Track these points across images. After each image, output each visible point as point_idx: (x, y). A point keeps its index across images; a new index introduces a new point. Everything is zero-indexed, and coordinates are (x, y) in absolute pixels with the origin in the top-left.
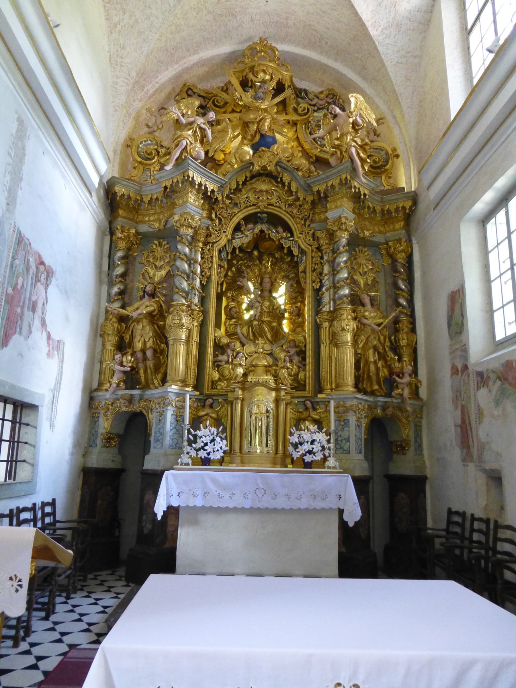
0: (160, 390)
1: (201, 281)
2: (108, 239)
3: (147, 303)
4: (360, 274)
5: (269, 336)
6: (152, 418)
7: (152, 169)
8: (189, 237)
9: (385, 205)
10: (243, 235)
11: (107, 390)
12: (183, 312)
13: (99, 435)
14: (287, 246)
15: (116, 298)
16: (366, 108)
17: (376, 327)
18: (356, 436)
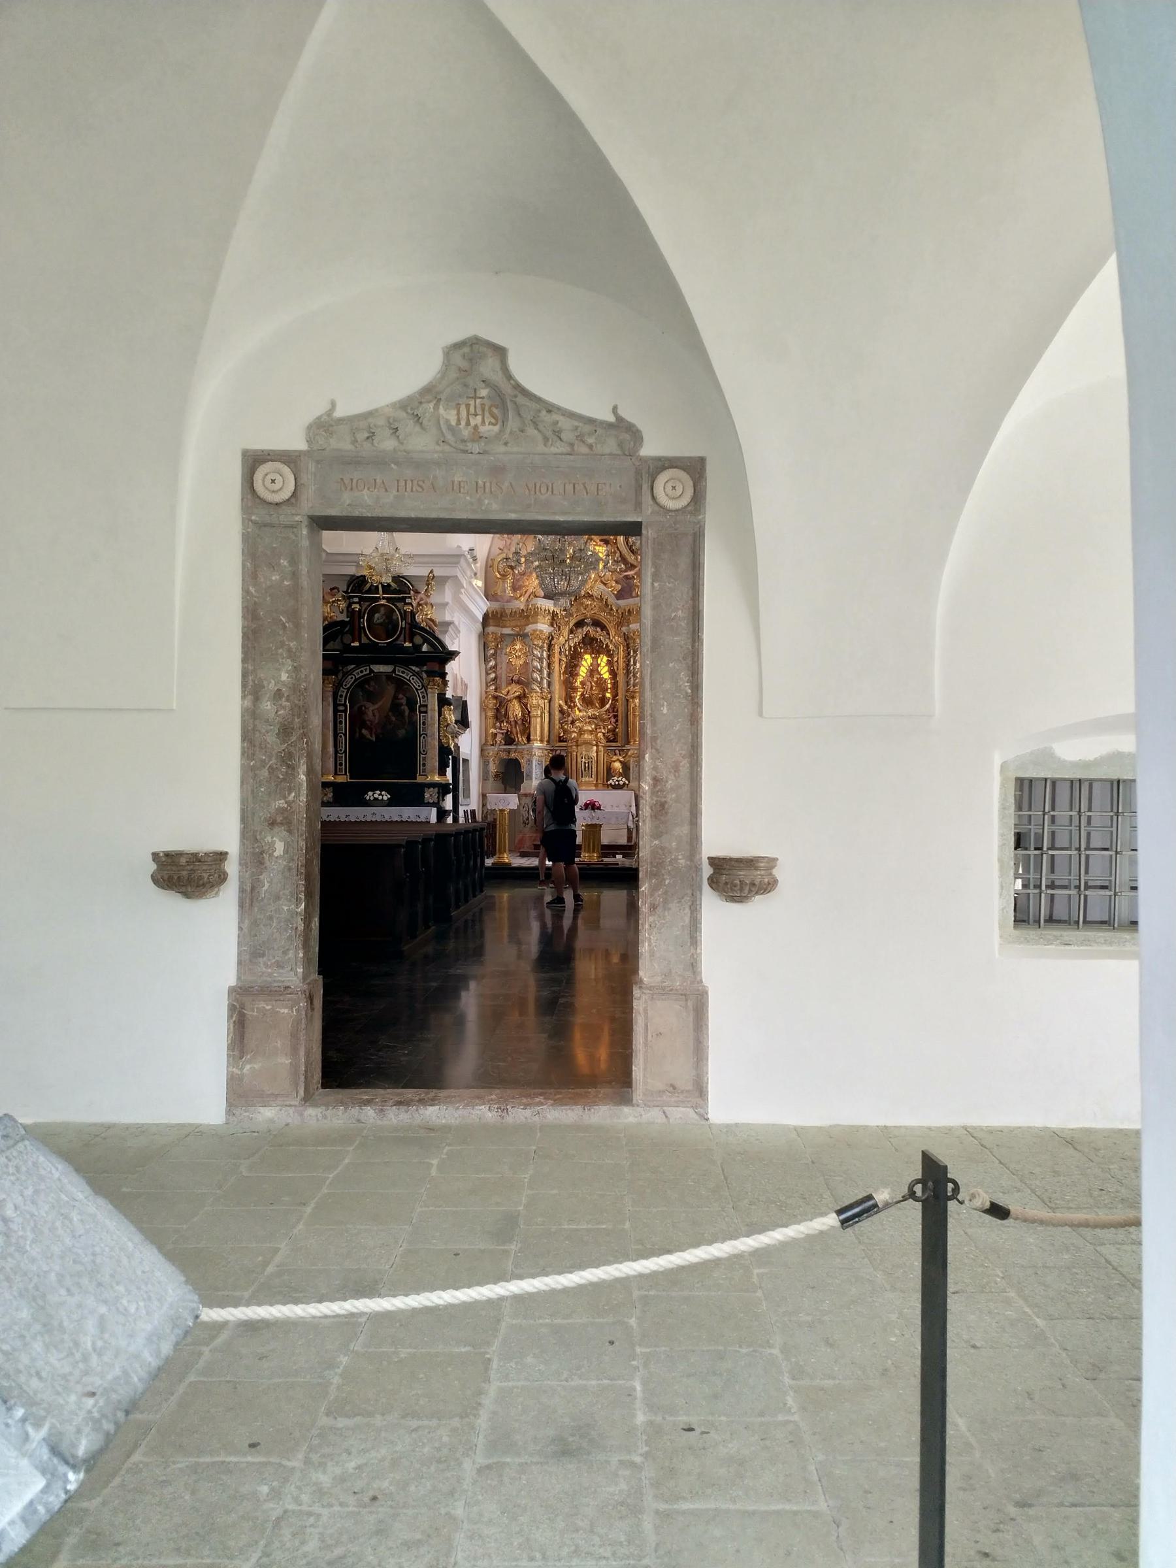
6: (523, 762)
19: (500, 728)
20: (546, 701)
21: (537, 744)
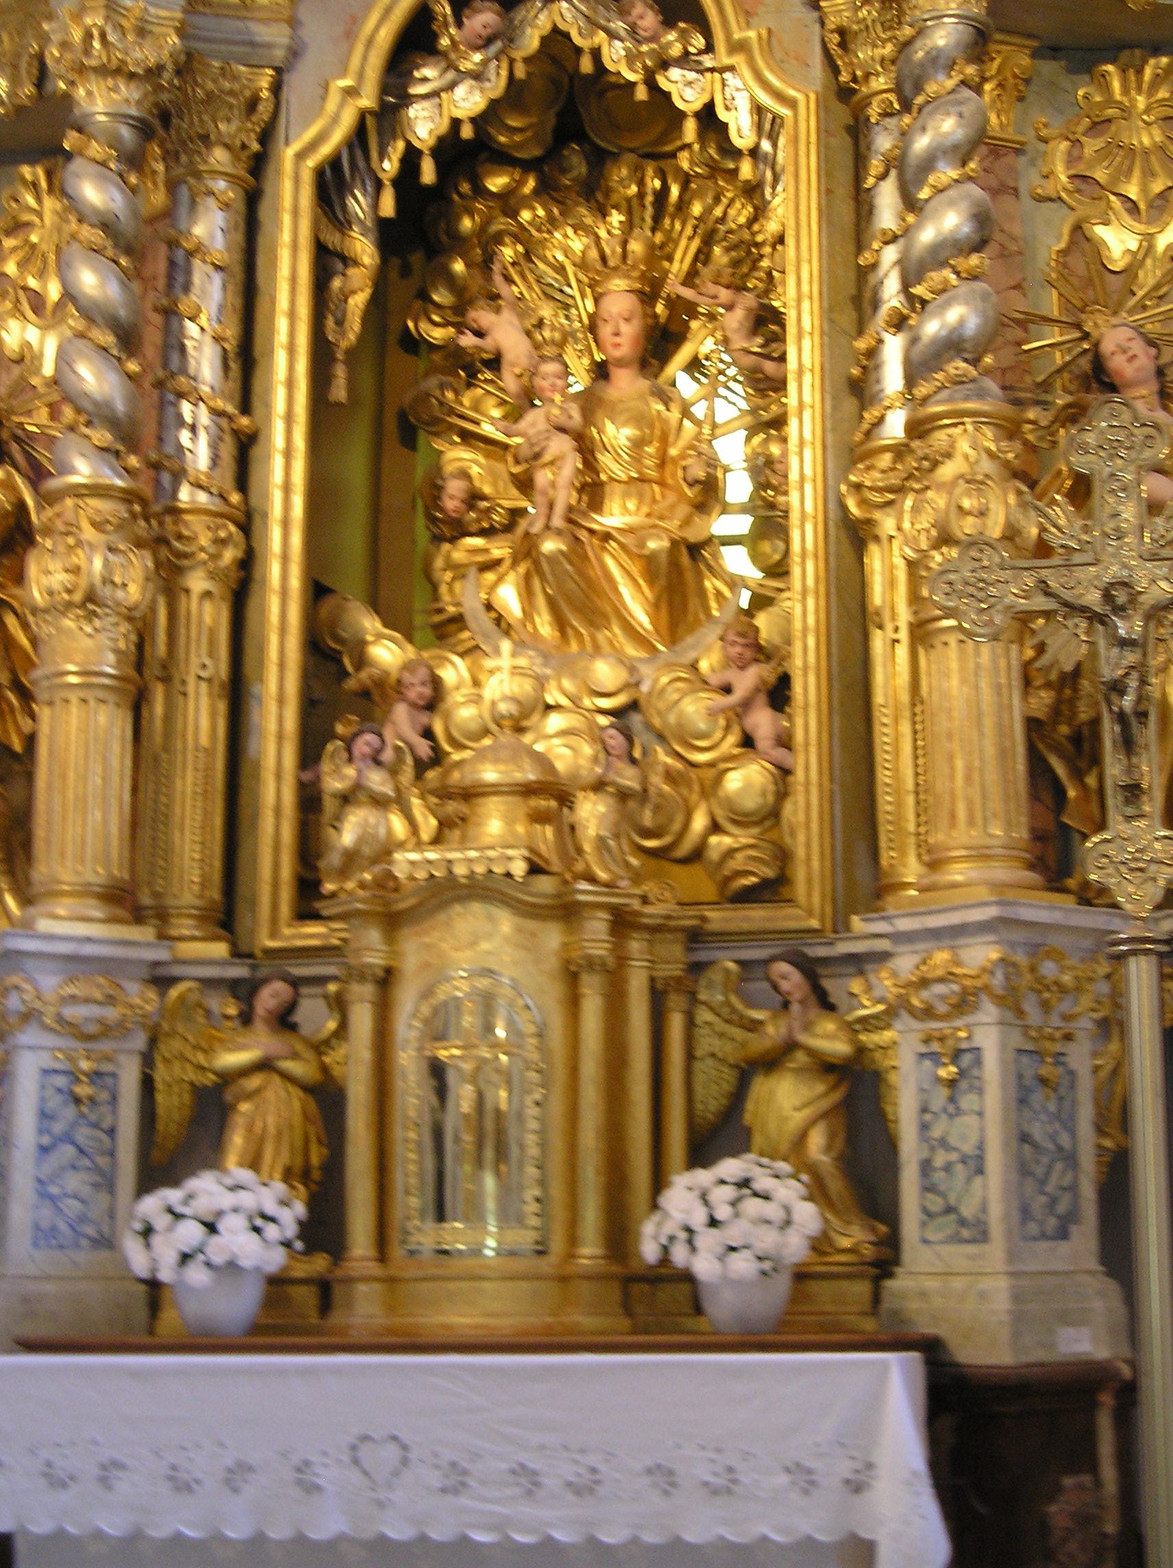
4: (1133, 208)
5: (641, 616)
8: (126, 133)
10: (451, 75)
14: (697, 105)
18: (1025, 1138)
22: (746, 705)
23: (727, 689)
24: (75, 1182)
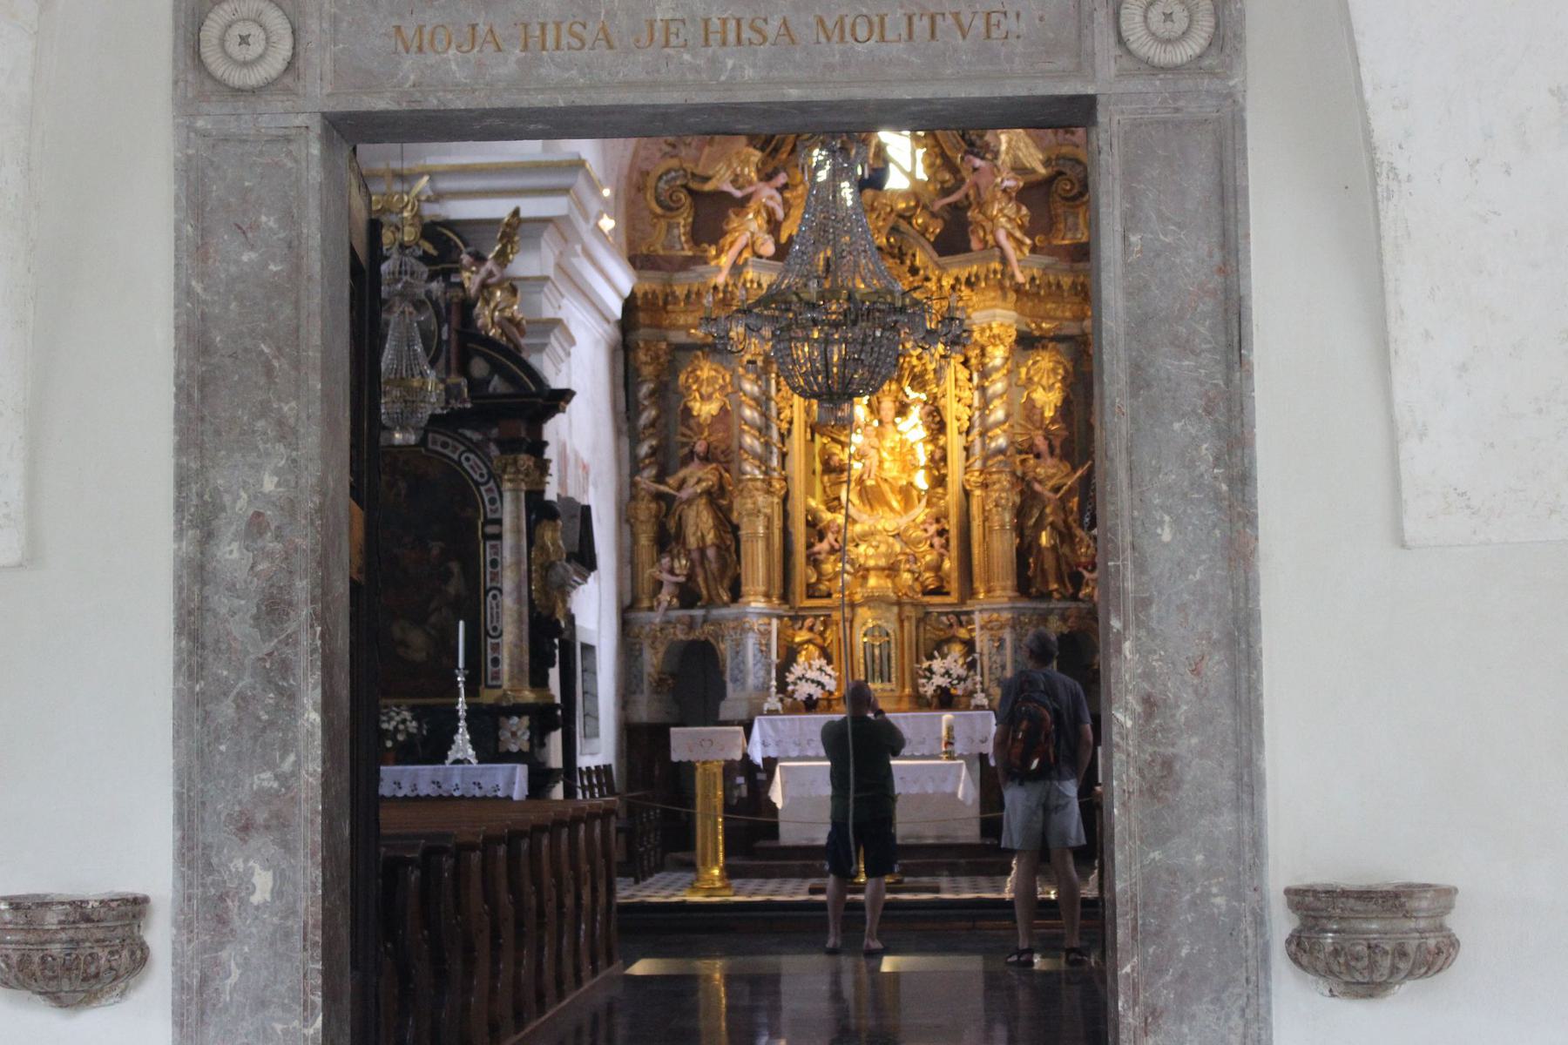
0: (733, 610)
1: (779, 429)
2: (621, 354)
3: (700, 474)
4: (1044, 389)
6: (725, 647)
7: (682, 222)
9: (1078, 276)
11: (651, 609)
12: (757, 490)
13: (645, 676)
15: (647, 461)
16: (1027, 147)
17: (1050, 495)
19: (671, 572)
20: (776, 500)
21: (757, 604)
22: (932, 536)
23: (926, 530)
24: (762, 673)
